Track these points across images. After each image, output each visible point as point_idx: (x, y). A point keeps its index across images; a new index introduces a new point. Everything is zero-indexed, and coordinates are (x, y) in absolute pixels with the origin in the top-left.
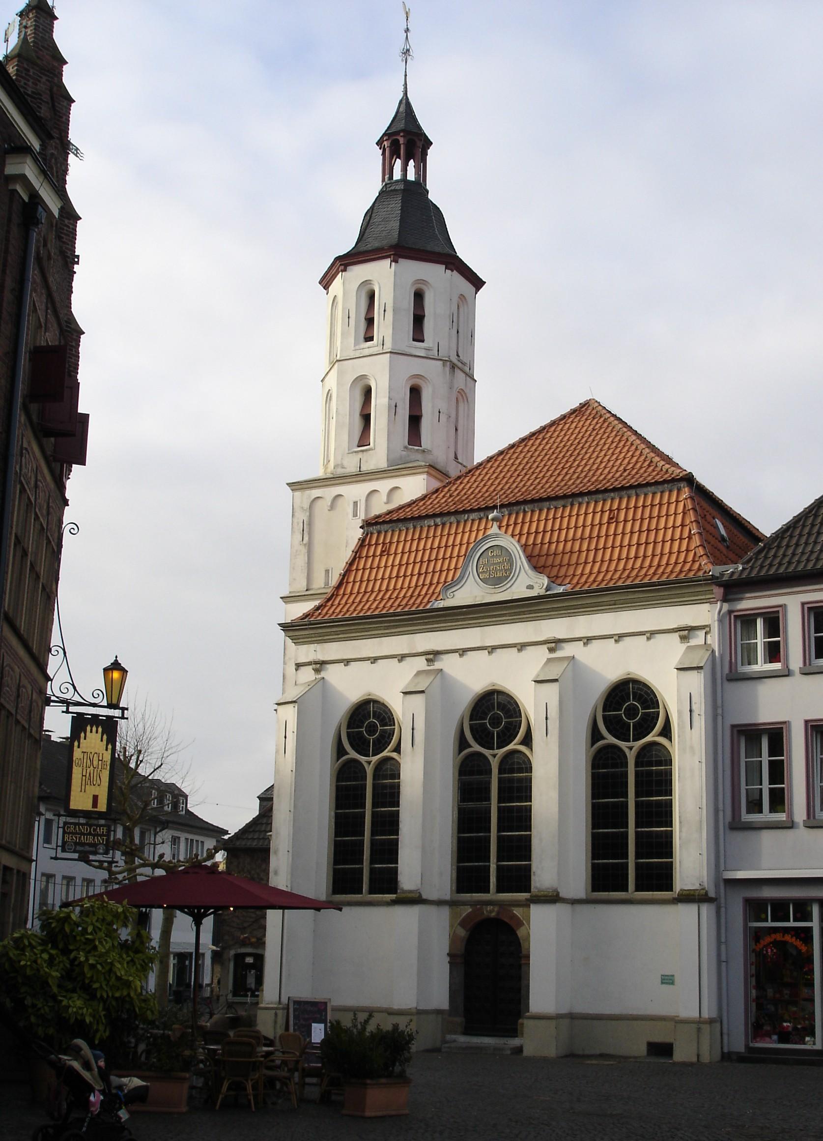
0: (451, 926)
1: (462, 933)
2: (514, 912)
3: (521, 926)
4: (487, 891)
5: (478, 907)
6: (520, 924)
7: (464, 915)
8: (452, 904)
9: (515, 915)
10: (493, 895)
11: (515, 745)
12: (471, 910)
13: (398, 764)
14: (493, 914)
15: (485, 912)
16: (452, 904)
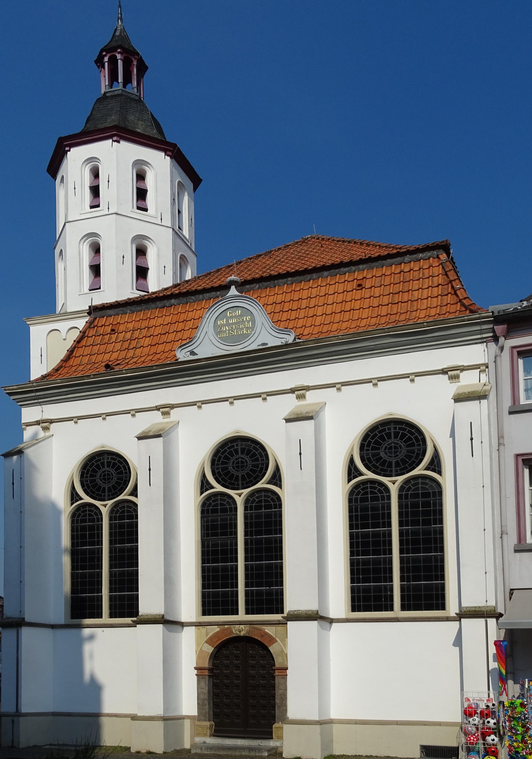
0: (198, 644)
1: (209, 649)
2: (266, 630)
3: (273, 643)
4: (235, 612)
5: (226, 626)
6: (273, 640)
7: (211, 635)
8: (198, 625)
9: (266, 634)
10: (242, 616)
11: (263, 483)
12: (218, 629)
13: (136, 505)
14: (242, 634)
15: (234, 631)
16: (198, 625)
